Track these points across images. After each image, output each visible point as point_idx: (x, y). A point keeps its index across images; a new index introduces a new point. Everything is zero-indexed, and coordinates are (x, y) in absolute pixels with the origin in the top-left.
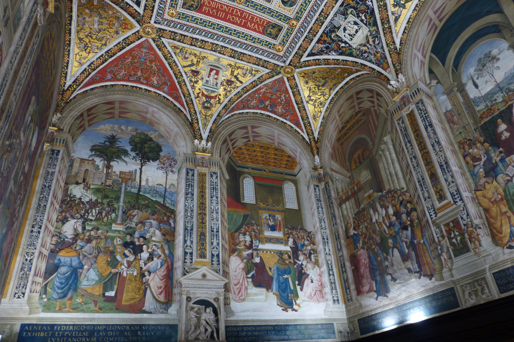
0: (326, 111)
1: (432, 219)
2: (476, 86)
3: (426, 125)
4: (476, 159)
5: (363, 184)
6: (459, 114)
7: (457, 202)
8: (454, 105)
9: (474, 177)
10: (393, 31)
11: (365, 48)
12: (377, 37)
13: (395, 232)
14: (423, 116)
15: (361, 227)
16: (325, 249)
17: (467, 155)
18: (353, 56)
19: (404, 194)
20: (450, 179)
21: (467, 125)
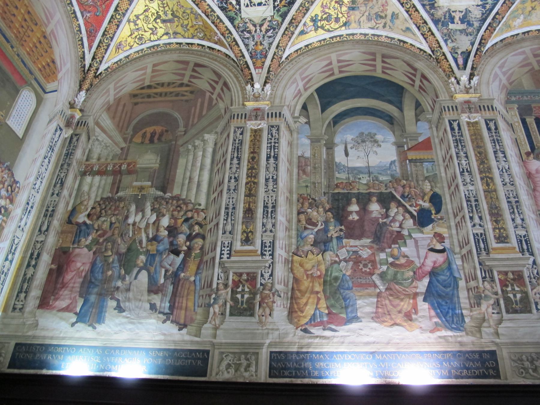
0: (138, 52)
1: (221, 258)
2: (347, 154)
3: (270, 154)
4: (310, 222)
5: (140, 168)
6: (315, 168)
7: (265, 255)
8: (314, 156)
9: (299, 238)
10: (292, 40)
11: (252, 28)
12: (274, 29)
13: (157, 251)
14: (271, 143)
15: (103, 219)
16: (21, 219)
17: (303, 213)
18: (232, 23)
19: (197, 211)
20: (269, 226)
21: (318, 183)
